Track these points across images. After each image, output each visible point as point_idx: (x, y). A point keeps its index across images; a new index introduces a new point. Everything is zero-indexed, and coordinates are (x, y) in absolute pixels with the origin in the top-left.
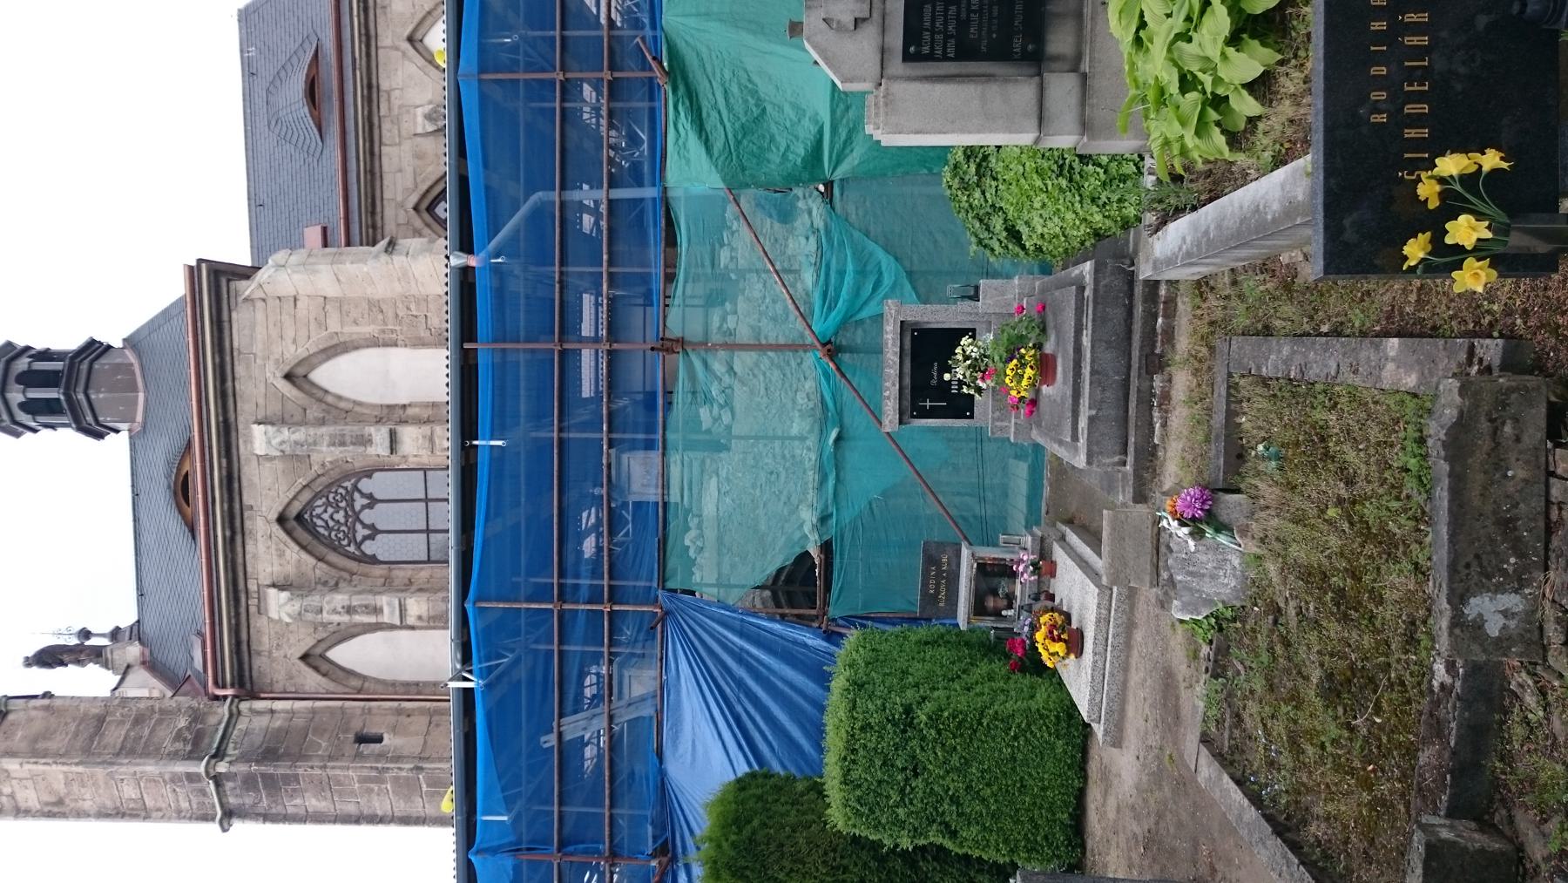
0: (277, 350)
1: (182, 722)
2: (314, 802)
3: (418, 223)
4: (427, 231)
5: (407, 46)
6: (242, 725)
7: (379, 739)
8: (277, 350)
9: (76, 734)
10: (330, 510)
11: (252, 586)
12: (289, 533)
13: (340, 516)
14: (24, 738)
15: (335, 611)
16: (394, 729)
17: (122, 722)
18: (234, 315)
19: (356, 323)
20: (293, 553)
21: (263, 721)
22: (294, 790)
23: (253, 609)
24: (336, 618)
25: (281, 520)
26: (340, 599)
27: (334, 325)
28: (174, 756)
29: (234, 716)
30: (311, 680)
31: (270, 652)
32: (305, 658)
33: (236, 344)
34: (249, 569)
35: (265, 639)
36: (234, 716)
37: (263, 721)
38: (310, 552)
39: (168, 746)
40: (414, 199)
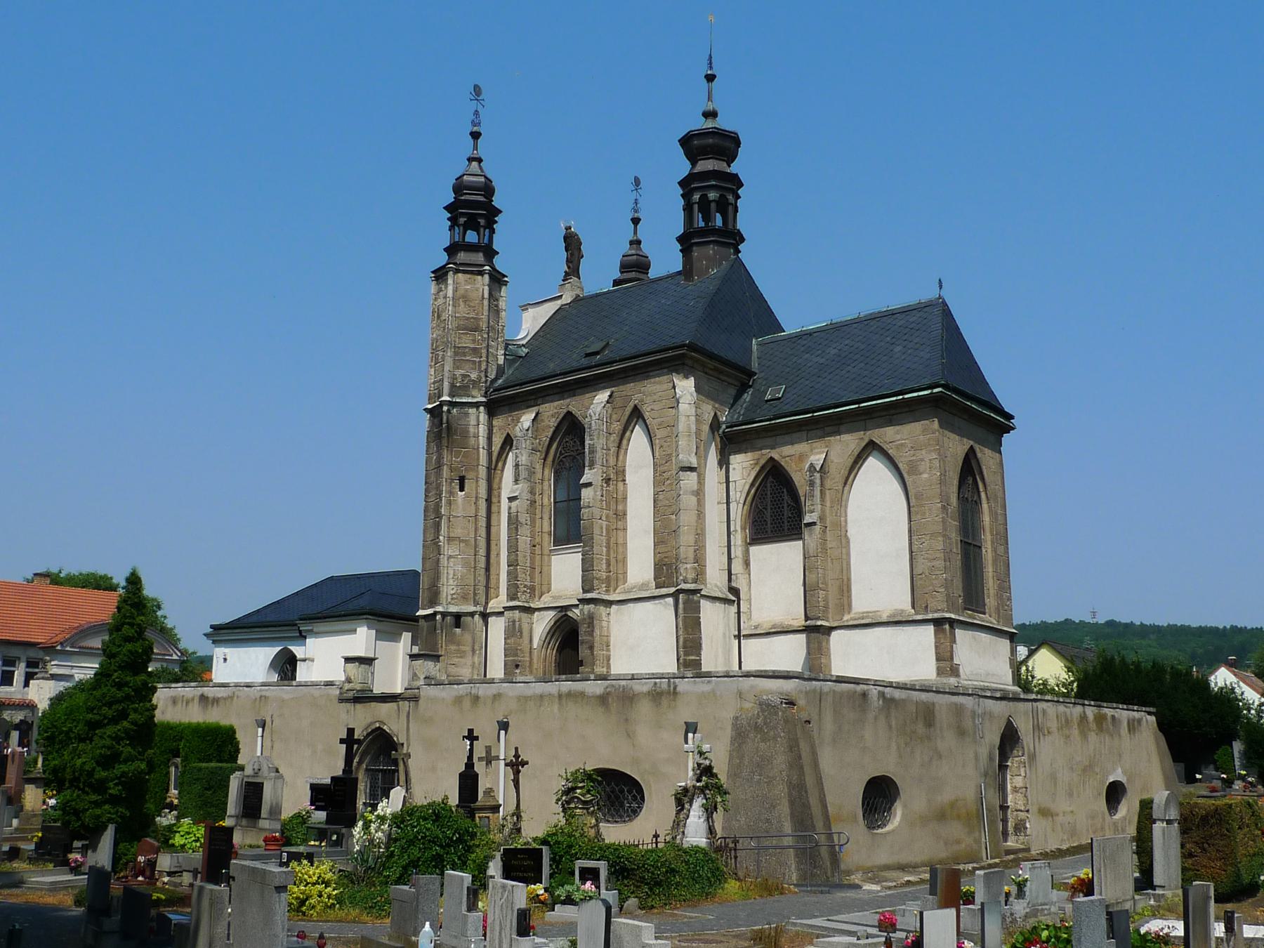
0: (648, 399)
1: (474, 376)
3: (762, 462)
4: (757, 468)
5: (866, 441)
6: (472, 411)
7: (462, 489)
8: (648, 399)
9: (468, 319)
12: (564, 418)
14: (466, 290)
16: (467, 496)
17: (474, 341)
20: (553, 423)
21: (473, 422)
25: (569, 413)
27: (660, 434)
28: (454, 378)
29: (476, 405)
30: (498, 441)
36: (476, 405)
37: (473, 422)
38: (554, 432)
39: (459, 372)
40: (776, 457)
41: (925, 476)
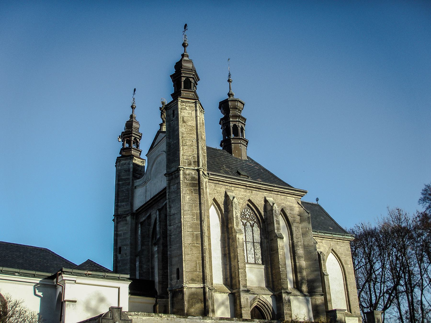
2: (188, 197)
10: (249, 214)
11: (233, 188)
13: (247, 216)
15: (236, 213)
18: (294, 198)
19: (296, 230)
22: (192, 192)
23: (227, 187)
24: (234, 213)
26: (239, 215)
31: (216, 190)
32: (214, 200)
33: (288, 197)
34: (237, 188)
35: (219, 189)
41: (349, 266)
